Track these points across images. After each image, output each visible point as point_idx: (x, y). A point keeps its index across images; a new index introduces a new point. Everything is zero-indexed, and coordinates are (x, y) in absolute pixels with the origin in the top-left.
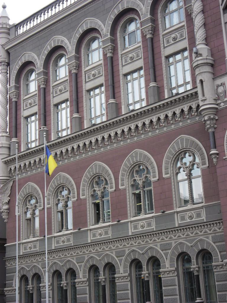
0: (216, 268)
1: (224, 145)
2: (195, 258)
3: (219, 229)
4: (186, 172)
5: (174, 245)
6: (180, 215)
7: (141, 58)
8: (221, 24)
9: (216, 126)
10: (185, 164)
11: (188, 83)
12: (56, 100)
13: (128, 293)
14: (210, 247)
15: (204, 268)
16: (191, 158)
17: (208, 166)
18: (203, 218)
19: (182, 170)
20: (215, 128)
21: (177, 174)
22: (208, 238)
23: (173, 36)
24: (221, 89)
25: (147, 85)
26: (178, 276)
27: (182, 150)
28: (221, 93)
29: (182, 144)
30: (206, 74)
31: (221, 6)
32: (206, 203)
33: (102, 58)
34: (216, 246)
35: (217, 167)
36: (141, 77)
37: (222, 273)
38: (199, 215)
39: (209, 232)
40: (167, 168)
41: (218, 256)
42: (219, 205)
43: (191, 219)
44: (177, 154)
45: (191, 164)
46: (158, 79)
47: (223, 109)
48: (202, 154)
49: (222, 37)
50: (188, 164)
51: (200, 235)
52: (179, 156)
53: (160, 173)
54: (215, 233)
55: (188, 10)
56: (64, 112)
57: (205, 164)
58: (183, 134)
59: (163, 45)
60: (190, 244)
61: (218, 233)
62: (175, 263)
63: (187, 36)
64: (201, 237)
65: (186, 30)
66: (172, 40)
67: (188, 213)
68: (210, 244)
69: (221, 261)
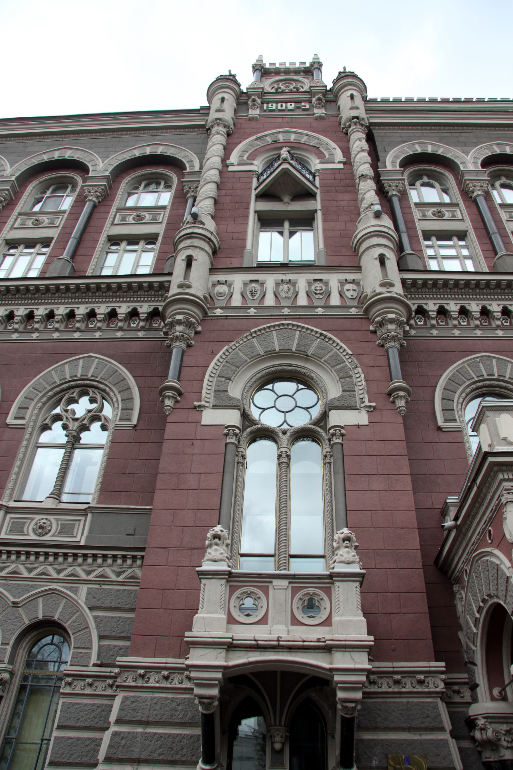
0: (70, 684)
1: (202, 381)
2: (11, 643)
6: (11, 518)
9: (193, 342)
14: (74, 618)
15: (25, 678)
17: (135, 426)
20: (189, 346)
27: (80, 382)
29: (86, 368)
30: (202, 252)
31: (253, 191)
34: (95, 618)
35: (169, 419)
37: (85, 701)
39: (84, 576)
40: (25, 406)
43: (40, 535)
44: (64, 386)
45: (90, 414)
46: (78, 259)
49: (247, 224)
54: (100, 583)
55: (184, 186)
57: (129, 420)
59: (111, 219)
60: (14, 597)
61: (112, 583)
63: (166, 219)
66: (134, 219)
67: (38, 517)
68: (77, 609)
69: (95, 665)
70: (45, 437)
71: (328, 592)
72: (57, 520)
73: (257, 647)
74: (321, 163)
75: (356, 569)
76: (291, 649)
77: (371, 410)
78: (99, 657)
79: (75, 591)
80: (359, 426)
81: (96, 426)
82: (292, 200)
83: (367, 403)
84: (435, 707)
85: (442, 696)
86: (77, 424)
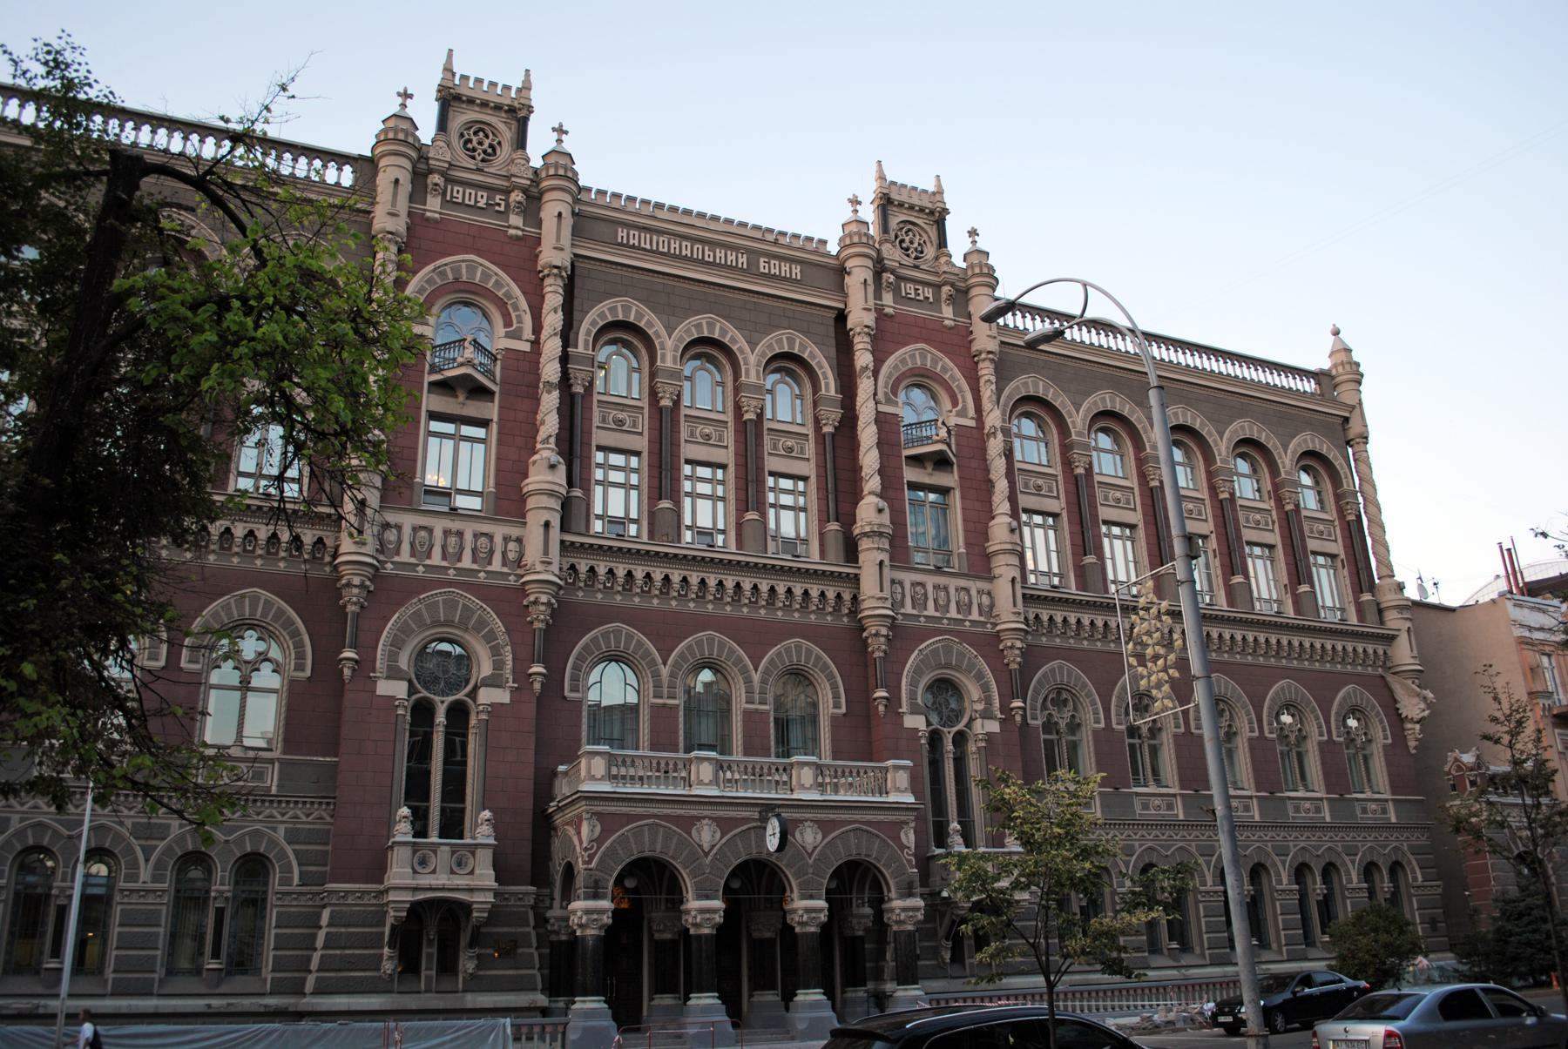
1: (376, 647)
3: (308, 816)
8: (420, 408)
13: (158, 934)
20: (362, 607)
22: (274, 829)
24: (391, 535)
28: (390, 543)
29: (253, 608)
32: (284, 752)
34: (294, 850)
35: (347, 687)
37: (293, 909)
42: (335, 765)
47: (389, 576)
49: (418, 435)
51: (254, 821)
54: (295, 823)
57: (303, 670)
58: (260, 587)
61: (303, 823)
71: (473, 854)
73: (431, 889)
74: (508, 335)
75: (492, 841)
76: (450, 890)
77: (513, 691)
78: (300, 879)
79: (274, 829)
80: (502, 704)
81: (266, 668)
82: (467, 398)
83: (511, 684)
84: (526, 913)
85: (533, 908)
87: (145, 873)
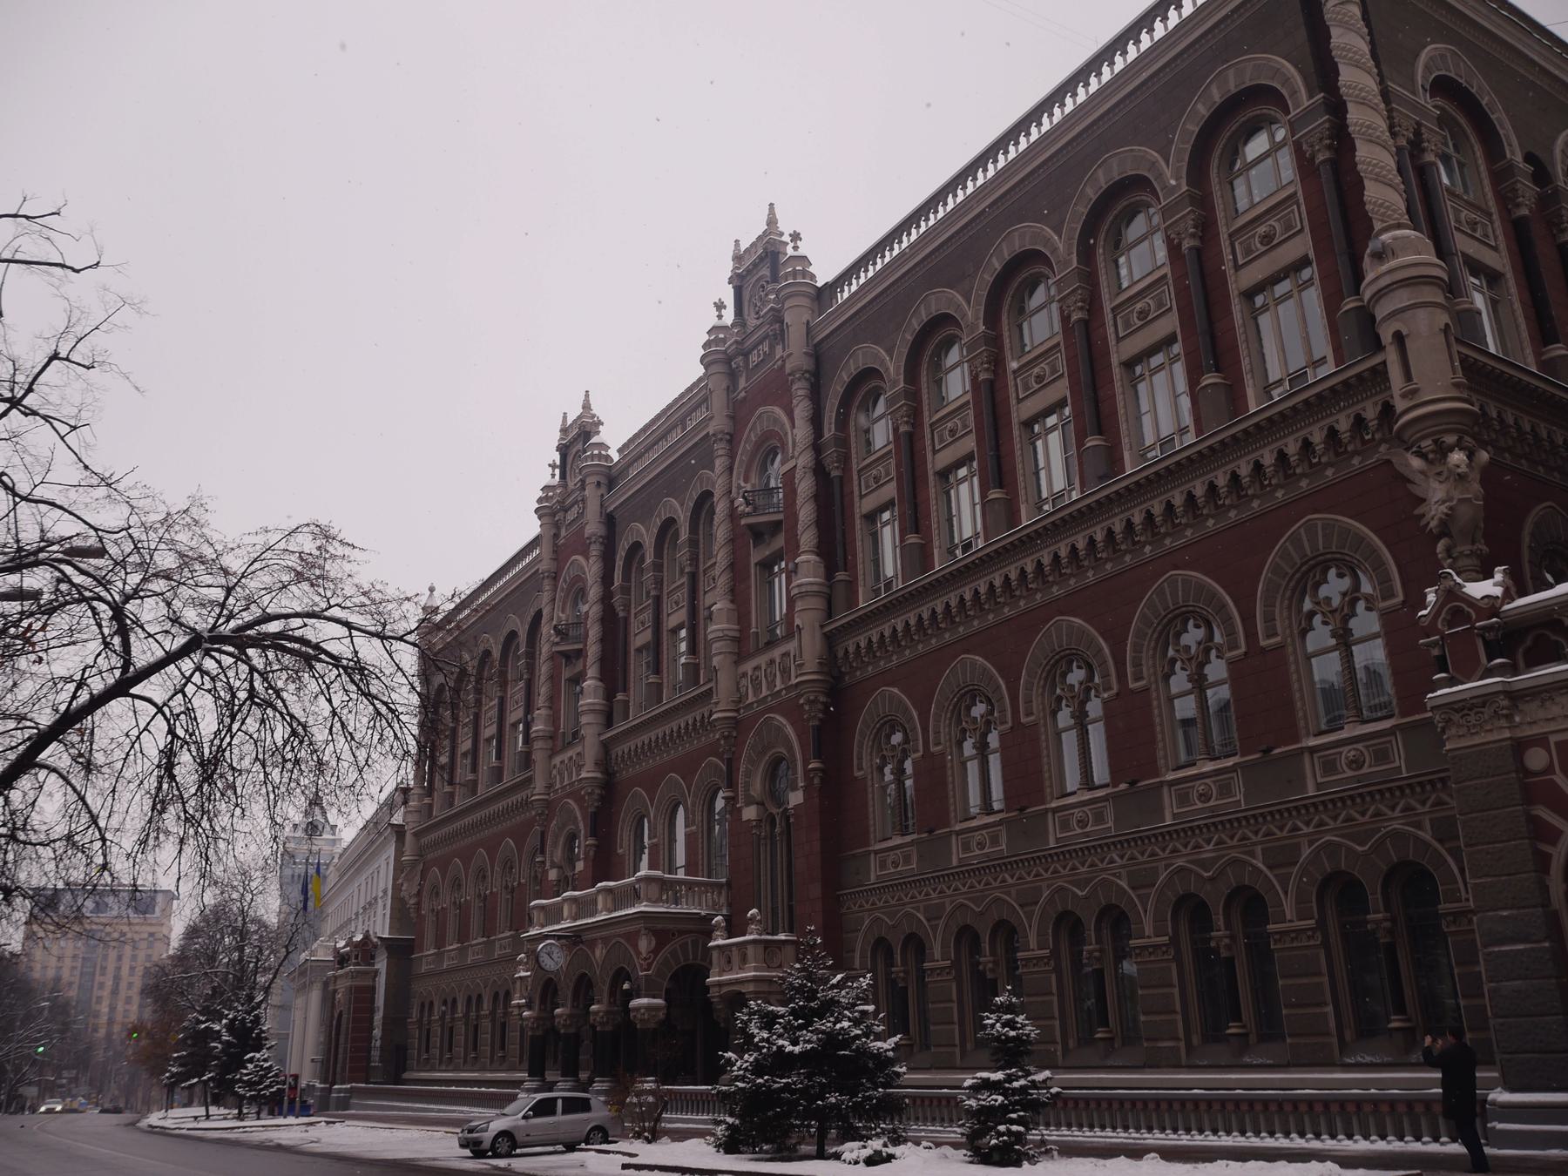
4: (1330, 627)
5: (1306, 852)
7: (1170, 309)
10: (1328, 600)
11: (1323, 360)
12: (944, 459)
16: (1346, 583)
18: (1397, 764)
19: (1317, 619)
21: (1304, 633)
22: (1419, 826)
23: (1262, 230)
25: (1193, 382)
26: (1326, 944)
33: (1057, 327)
36: (1176, 359)
38: (1382, 756)
41: (1457, 882)
48: (1379, 567)
50: (1336, 602)
52: (1310, 575)
53: (1251, 635)
56: (964, 488)
57: (1393, 595)
62: (1314, 905)
64: (1396, 825)
65: (1303, 208)
66: (1261, 243)
67: (1346, 749)
68: (1427, 845)
70: (1313, 641)
72: (1367, 747)
86: (1338, 616)
87: (1289, 909)
